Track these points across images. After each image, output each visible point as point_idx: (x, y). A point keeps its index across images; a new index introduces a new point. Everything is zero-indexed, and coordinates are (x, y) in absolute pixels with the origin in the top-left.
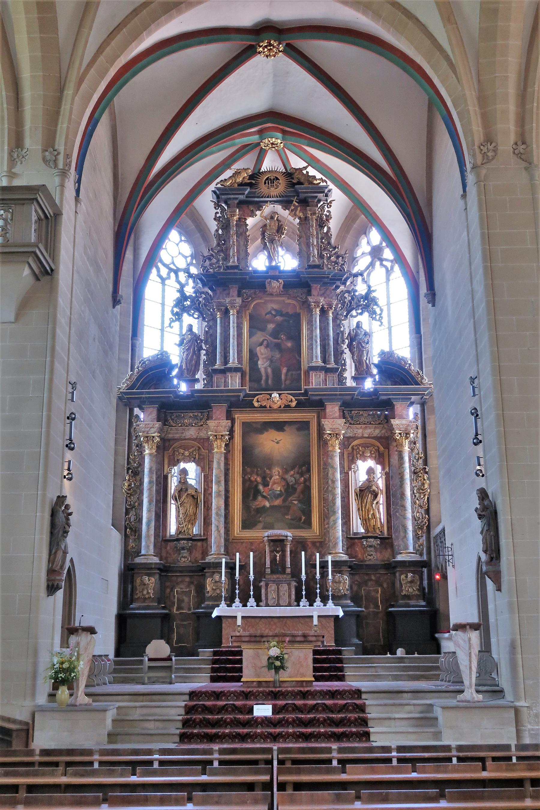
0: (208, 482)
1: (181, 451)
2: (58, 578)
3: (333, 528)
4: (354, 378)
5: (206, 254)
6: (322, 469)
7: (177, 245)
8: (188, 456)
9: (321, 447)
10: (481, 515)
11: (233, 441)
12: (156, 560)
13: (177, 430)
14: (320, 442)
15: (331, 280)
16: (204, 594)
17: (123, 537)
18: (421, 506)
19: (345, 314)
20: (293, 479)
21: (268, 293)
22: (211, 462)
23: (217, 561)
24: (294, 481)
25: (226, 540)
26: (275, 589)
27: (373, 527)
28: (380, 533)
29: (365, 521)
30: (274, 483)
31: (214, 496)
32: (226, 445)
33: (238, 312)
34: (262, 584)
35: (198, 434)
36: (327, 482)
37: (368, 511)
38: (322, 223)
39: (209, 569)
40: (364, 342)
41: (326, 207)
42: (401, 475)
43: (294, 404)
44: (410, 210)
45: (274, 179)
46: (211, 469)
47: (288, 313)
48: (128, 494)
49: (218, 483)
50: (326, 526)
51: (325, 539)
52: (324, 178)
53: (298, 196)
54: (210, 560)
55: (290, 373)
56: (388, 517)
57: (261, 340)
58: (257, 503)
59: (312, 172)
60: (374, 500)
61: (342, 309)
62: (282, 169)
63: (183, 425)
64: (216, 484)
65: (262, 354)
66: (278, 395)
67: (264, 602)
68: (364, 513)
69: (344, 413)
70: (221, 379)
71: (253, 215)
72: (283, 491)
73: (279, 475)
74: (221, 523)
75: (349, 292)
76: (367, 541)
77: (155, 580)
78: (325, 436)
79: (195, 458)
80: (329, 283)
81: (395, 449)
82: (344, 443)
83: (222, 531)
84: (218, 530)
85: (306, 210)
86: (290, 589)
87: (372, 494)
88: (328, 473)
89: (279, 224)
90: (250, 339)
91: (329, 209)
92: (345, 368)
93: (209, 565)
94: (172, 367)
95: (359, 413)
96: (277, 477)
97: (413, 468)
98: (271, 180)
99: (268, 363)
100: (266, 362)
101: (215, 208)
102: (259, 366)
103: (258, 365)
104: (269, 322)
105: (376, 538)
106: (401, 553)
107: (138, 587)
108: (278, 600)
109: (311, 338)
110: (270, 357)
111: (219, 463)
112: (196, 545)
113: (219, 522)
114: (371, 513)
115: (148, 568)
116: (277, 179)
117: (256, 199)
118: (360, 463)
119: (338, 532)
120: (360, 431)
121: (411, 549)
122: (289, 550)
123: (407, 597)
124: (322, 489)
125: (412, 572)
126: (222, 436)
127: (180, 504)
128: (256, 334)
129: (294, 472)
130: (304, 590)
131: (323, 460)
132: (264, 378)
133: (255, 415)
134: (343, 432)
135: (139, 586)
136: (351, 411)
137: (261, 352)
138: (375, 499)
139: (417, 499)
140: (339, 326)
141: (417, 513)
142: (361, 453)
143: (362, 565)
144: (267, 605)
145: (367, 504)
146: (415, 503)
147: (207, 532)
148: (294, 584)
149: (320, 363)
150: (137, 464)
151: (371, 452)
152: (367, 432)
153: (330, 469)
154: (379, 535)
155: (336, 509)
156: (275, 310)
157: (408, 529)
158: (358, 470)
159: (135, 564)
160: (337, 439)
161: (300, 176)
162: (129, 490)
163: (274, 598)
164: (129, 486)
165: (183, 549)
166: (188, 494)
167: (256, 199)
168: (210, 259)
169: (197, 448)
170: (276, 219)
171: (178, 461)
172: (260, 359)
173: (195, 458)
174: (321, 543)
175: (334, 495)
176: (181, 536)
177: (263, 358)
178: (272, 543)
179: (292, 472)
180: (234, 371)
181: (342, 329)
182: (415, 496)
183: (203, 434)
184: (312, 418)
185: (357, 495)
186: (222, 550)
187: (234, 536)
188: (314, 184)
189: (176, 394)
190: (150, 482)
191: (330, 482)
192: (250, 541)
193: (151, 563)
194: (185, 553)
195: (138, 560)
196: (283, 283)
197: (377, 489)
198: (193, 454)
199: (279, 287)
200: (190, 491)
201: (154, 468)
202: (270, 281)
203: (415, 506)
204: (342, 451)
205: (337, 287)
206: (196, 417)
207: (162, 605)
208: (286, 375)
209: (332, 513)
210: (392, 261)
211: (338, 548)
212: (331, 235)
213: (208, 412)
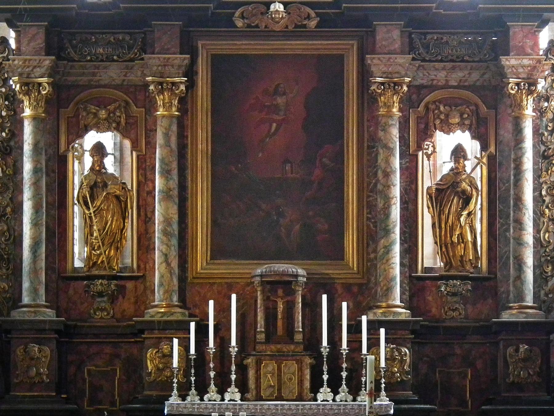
0: (145, 169)
1: (93, 109)
3: (384, 261)
6: (366, 148)
9: (366, 105)
11: (192, 91)
12: (50, 314)
14: (363, 97)
16: (141, 378)
22: (150, 132)
23: (165, 318)
25: (182, 279)
26: (274, 369)
27: (459, 258)
28: (472, 270)
31: (159, 199)
32: (182, 101)
34: (250, 361)
35: (125, 76)
36: (376, 174)
37: (452, 230)
39: (153, 334)
42: (518, 163)
46: (151, 145)
49: (166, 173)
54: (152, 316)
60: (463, 208)
63: (97, 58)
64: (162, 174)
67: (254, 393)
68: (443, 233)
74: (173, 248)
77: (52, 351)
79: (118, 124)
81: (509, 111)
82: (410, 97)
83: (175, 264)
84: (168, 264)
86: (300, 369)
87: (460, 198)
88: (376, 155)
93: (151, 326)
95: (442, 39)
97: (543, 148)
105: (463, 278)
106: (511, 308)
108: (279, 390)
111: (167, 136)
114: (457, 233)
118: (440, 137)
119: (392, 268)
120: (442, 75)
121: (529, 300)
122: (300, 300)
123: (517, 386)
124: (365, 185)
127: (94, 212)
130: (325, 373)
131: (368, 131)
133: (238, 43)
136: (425, 34)
138: (466, 207)
139: (547, 207)
141: (545, 233)
142: (442, 117)
143: (437, 327)
144: (259, 398)
145: (451, 216)
146: (543, 214)
147: (145, 263)
148: (308, 361)
150: (7, 134)
151: (461, 116)
152: (455, 78)
154: (471, 273)
155: (392, 226)
157: (525, 263)
158: (434, 152)
159: (13, 322)
163: (271, 386)
165: (100, 294)
169: (123, 104)
175: (388, 200)
176: (95, 272)
178: (268, 287)
182: (544, 201)
183: (134, 77)
184: (349, 49)
185: (431, 197)
186: (175, 298)
191: (380, 174)
193: (44, 322)
194: (103, 302)
195: (16, 315)
197: (469, 188)
198: (115, 114)
200: (113, 189)
203: (542, 219)
206: (119, 44)
207: (63, 396)
209: (383, 233)
211: (392, 297)
213: (145, 34)
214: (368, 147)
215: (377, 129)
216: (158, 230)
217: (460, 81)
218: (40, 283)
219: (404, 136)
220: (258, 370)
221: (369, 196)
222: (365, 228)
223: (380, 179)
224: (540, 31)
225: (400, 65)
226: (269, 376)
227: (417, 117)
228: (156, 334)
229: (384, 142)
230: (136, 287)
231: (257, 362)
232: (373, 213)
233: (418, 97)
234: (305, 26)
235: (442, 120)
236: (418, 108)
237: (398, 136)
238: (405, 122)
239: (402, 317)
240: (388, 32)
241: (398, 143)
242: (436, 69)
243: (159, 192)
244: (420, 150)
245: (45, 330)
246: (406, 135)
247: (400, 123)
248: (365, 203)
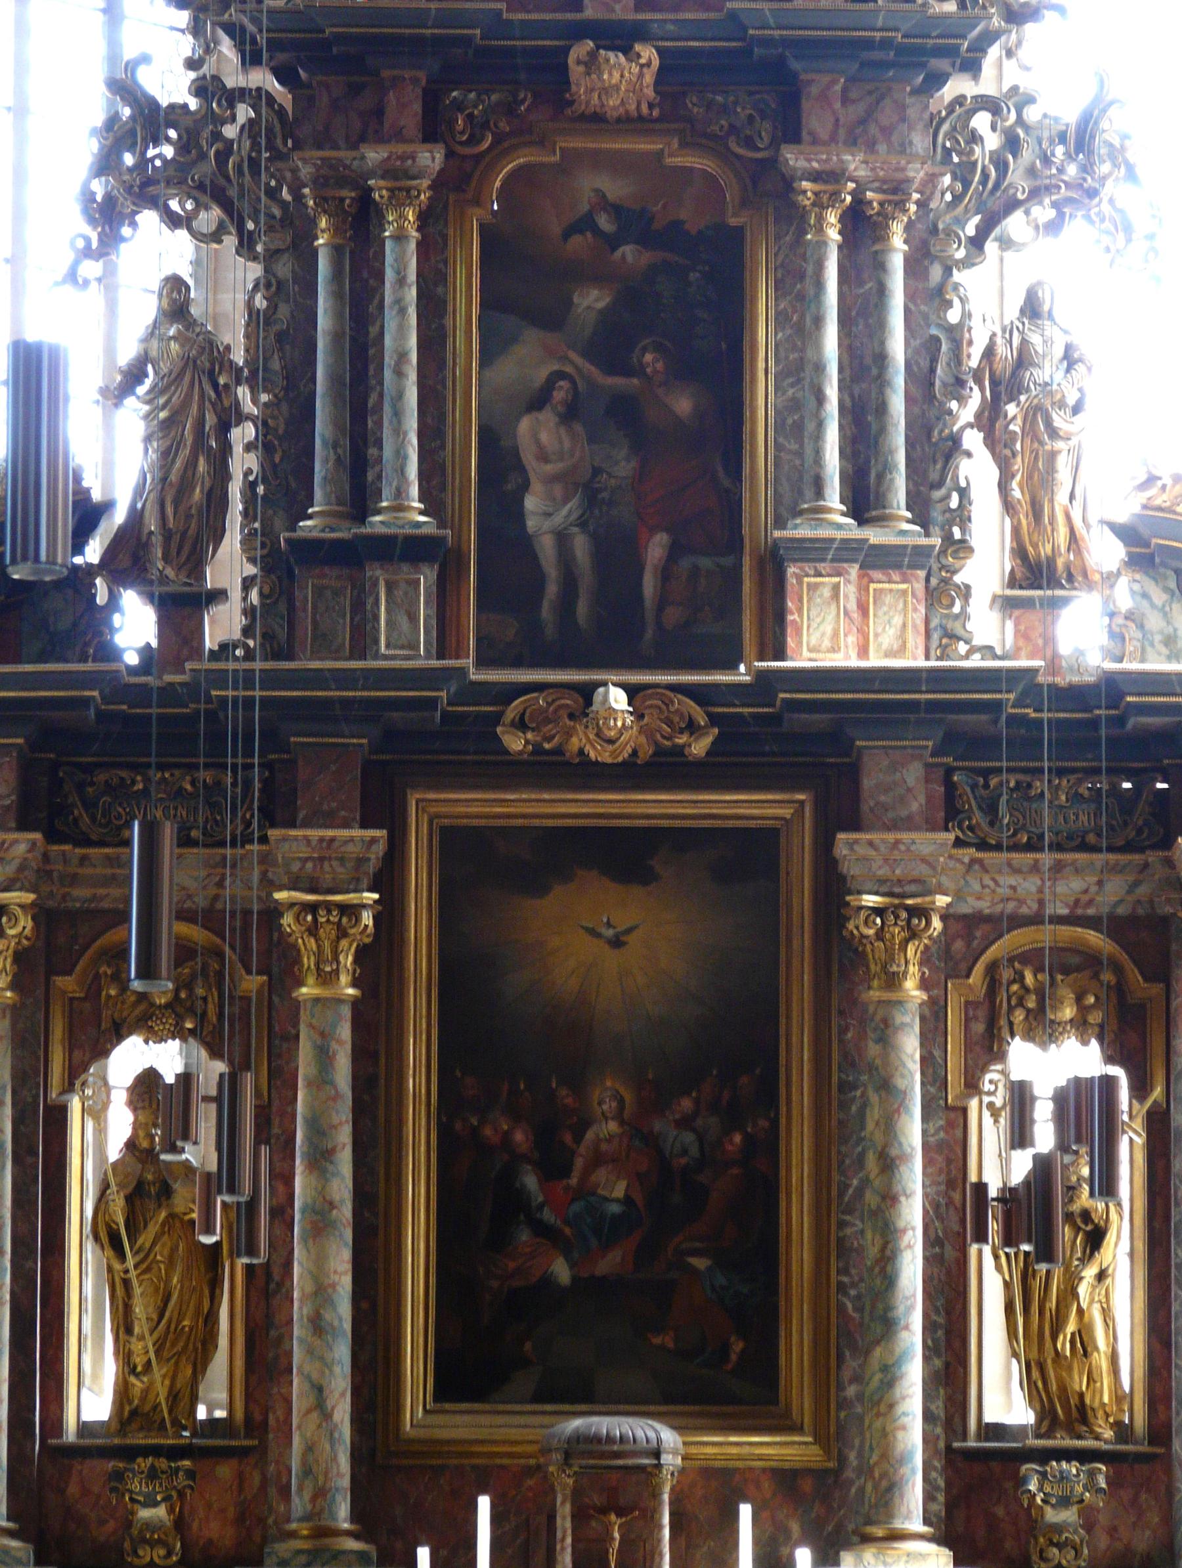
4: (1007, 605)
9: (835, 968)
19: (970, 230)
20: (689, 1138)
24: (694, 1151)
30: (597, 1160)
31: (303, 1230)
47: (677, 224)
55: (685, 563)
56: (1158, 1346)
57: (543, 373)
58: (512, 1265)
61: (957, 199)
65: (543, 457)
69: (950, 786)
72: (638, 1198)
73: (619, 1117)
75: (992, 105)
90: (487, 373)
92: (963, 541)
95: (1029, 786)
96: (613, 1126)
100: (566, 501)
102: (531, 524)
103: (518, 515)
120: (1029, 885)
124: (834, 1192)
128: (514, 340)
129: (697, 1102)
132: (552, 589)
136: (986, 773)
137: (537, 442)
140: (940, 297)
142: (1031, 1003)
151: (1079, 999)
156: (617, 210)
172: (536, 486)
179: (686, 1104)
180: (404, 558)
181: (953, 316)
205: (937, 80)
208: (666, 574)
215: (862, 1036)
216: (301, 1318)
217: (1077, 901)
219: (931, 1053)
222: (834, 1313)
223: (872, 1176)
225: (923, 860)
227: (967, 1003)
229: (882, 1072)
230: (241, 1477)
232: (853, 1271)
233: (968, 945)
234: (679, 751)
236: (968, 976)
237: (917, 1056)
238: (936, 1015)
240: (894, 767)
241: (918, 1077)
242: (1017, 871)
243: (303, 1211)
244: (971, 1096)
246: (937, 1053)
247: (923, 1019)
248: (833, 1245)
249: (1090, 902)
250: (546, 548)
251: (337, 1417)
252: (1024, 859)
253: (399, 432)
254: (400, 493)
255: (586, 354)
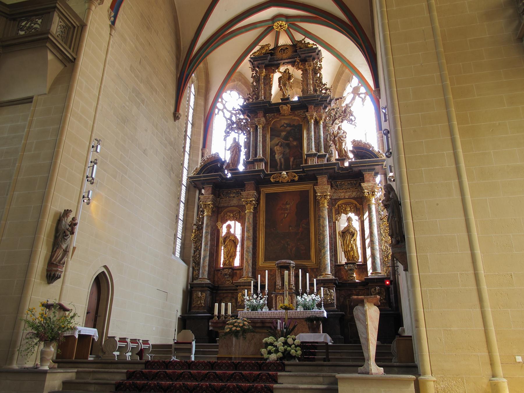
1: (228, 214)
2: (55, 269)
5: (247, 97)
6: (317, 220)
7: (230, 94)
8: (232, 217)
10: (387, 205)
13: (225, 200)
15: (320, 101)
17: (191, 269)
18: (386, 242)
19: (331, 123)
21: (282, 114)
23: (245, 281)
26: (282, 299)
27: (352, 256)
29: (347, 253)
32: (255, 209)
33: (263, 127)
35: (239, 202)
37: (348, 246)
38: (316, 71)
40: (343, 137)
41: (318, 62)
43: (296, 178)
44: (361, 41)
45: (285, 49)
48: (194, 241)
49: (248, 231)
50: (321, 258)
51: (320, 267)
52: (315, 43)
53: (300, 57)
55: (295, 160)
57: (278, 142)
59: (307, 40)
61: (329, 120)
62: (290, 43)
64: (246, 232)
65: (278, 151)
66: (285, 173)
70: (252, 167)
71: (274, 72)
76: (348, 266)
78: (318, 197)
80: (319, 104)
83: (250, 262)
84: (248, 262)
85: (305, 63)
87: (350, 234)
89: (289, 75)
90: (271, 143)
91: (321, 63)
94: (223, 163)
97: (380, 216)
98: (283, 50)
99: (281, 156)
101: (252, 71)
102: (276, 158)
103: (275, 157)
104: (282, 131)
107: (195, 299)
109: (309, 139)
110: (283, 152)
111: (249, 218)
112: (236, 273)
113: (248, 256)
114: (350, 247)
115: (202, 287)
116: (287, 48)
117: (275, 62)
120: (343, 194)
124: (317, 233)
125: (379, 286)
126: (251, 201)
132: (279, 165)
134: (329, 194)
135: (196, 298)
136: (336, 182)
139: (384, 237)
141: (383, 247)
142: (344, 209)
146: (382, 240)
149: (314, 151)
151: (350, 208)
152: (347, 195)
153: (321, 219)
155: (326, 245)
156: (287, 124)
160: (325, 199)
161: (300, 45)
162: (195, 238)
164: (195, 236)
165: (226, 274)
166: (230, 239)
167: (275, 62)
168: (248, 100)
169: (238, 212)
170: (287, 72)
171: (227, 221)
172: (277, 154)
173: (237, 218)
174: (317, 269)
175: (324, 236)
176: (225, 267)
177: (278, 153)
182: (382, 235)
185: (340, 235)
186: (250, 275)
187: (259, 266)
188: (309, 47)
189: (227, 179)
190: (206, 232)
192: (270, 269)
196: (290, 107)
199: (288, 110)
201: (209, 224)
202: (282, 106)
203: (382, 242)
204: (331, 208)
206: (238, 193)
208: (293, 162)
210: (364, 93)
212: (322, 77)
214: (318, 220)
218: (205, 270)
220: (276, 299)
221: (319, 237)
224: (376, 177)
226: (280, 301)
228: (242, 287)
231: (275, 297)
235: (344, 210)
239: (331, 278)
245: (204, 287)
246: (331, 215)
249: (351, 196)
250: (278, 161)
251: (249, 262)
252: (341, 191)
253: (260, 149)
254: (260, 155)
255: (283, 139)
